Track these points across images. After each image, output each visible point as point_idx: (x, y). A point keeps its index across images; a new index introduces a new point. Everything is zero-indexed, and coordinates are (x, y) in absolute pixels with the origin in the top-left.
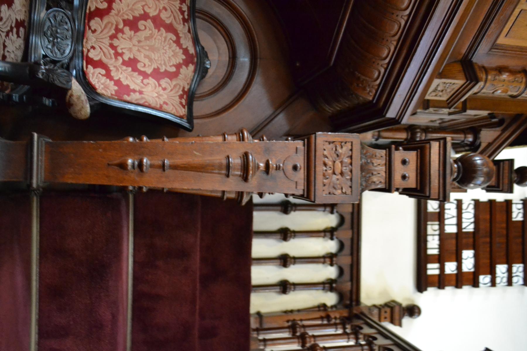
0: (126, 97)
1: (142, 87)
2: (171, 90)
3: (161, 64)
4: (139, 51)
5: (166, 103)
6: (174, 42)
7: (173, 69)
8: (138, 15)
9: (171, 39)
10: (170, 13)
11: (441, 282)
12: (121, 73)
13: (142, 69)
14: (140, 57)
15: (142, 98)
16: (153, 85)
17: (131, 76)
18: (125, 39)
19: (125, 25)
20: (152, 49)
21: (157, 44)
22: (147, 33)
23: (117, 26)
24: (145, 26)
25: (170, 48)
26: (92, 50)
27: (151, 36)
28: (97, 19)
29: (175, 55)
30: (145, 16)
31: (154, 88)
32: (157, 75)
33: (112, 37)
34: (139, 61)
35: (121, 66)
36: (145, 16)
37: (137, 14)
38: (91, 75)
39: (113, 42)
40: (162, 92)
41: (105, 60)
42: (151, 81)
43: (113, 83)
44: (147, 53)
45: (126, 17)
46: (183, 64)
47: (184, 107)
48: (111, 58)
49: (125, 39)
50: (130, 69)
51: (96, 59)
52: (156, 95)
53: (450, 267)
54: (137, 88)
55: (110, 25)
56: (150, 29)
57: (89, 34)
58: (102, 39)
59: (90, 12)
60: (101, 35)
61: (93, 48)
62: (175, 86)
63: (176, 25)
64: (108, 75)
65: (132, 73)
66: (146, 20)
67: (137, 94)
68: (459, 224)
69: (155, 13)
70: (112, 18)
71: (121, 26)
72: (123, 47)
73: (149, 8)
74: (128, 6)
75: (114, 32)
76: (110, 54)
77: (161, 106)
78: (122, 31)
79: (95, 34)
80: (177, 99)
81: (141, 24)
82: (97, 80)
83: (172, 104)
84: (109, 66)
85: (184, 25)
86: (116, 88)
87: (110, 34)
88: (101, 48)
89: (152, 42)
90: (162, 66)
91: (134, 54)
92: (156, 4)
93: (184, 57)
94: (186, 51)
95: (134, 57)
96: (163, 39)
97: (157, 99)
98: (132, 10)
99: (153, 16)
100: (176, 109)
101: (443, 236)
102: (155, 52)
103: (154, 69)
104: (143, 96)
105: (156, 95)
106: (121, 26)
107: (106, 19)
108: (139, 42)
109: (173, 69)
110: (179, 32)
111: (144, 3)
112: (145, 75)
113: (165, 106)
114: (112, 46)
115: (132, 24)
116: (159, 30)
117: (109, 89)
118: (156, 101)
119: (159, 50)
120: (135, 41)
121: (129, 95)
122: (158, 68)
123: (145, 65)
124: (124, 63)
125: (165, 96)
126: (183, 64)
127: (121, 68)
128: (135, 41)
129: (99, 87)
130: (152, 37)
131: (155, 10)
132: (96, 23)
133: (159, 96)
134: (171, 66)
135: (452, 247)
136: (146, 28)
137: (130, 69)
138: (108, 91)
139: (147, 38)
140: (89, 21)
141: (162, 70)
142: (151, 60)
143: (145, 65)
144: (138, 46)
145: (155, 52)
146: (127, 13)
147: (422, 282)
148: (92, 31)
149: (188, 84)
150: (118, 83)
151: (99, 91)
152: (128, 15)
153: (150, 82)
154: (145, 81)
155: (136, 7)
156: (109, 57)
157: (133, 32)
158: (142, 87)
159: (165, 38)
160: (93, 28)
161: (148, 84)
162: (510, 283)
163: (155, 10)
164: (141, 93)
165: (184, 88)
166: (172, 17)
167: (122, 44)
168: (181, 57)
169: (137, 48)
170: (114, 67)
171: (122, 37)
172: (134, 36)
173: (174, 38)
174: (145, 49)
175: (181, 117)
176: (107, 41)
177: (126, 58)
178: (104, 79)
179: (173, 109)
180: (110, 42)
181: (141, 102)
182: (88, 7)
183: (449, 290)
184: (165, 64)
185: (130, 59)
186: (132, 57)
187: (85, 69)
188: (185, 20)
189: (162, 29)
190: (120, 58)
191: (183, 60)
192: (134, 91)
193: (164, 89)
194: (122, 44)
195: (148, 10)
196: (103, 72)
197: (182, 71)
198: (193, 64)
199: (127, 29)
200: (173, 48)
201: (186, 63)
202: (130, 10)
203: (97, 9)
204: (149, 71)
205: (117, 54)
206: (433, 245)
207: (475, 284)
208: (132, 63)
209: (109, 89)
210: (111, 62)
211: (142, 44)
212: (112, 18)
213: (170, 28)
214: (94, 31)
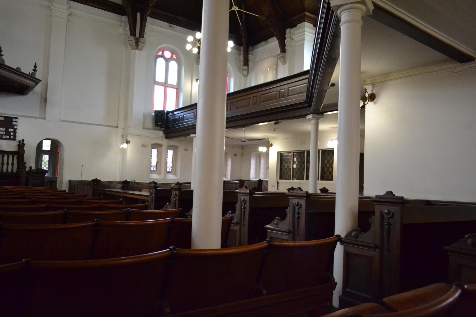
11: (15, 136)
53: (12, 134)
68: (3, 131)
101: (6, 135)
135: (8, 133)
147: (14, 139)
162: (16, 122)
183: (17, 134)
206: (7, 137)
207: (16, 129)
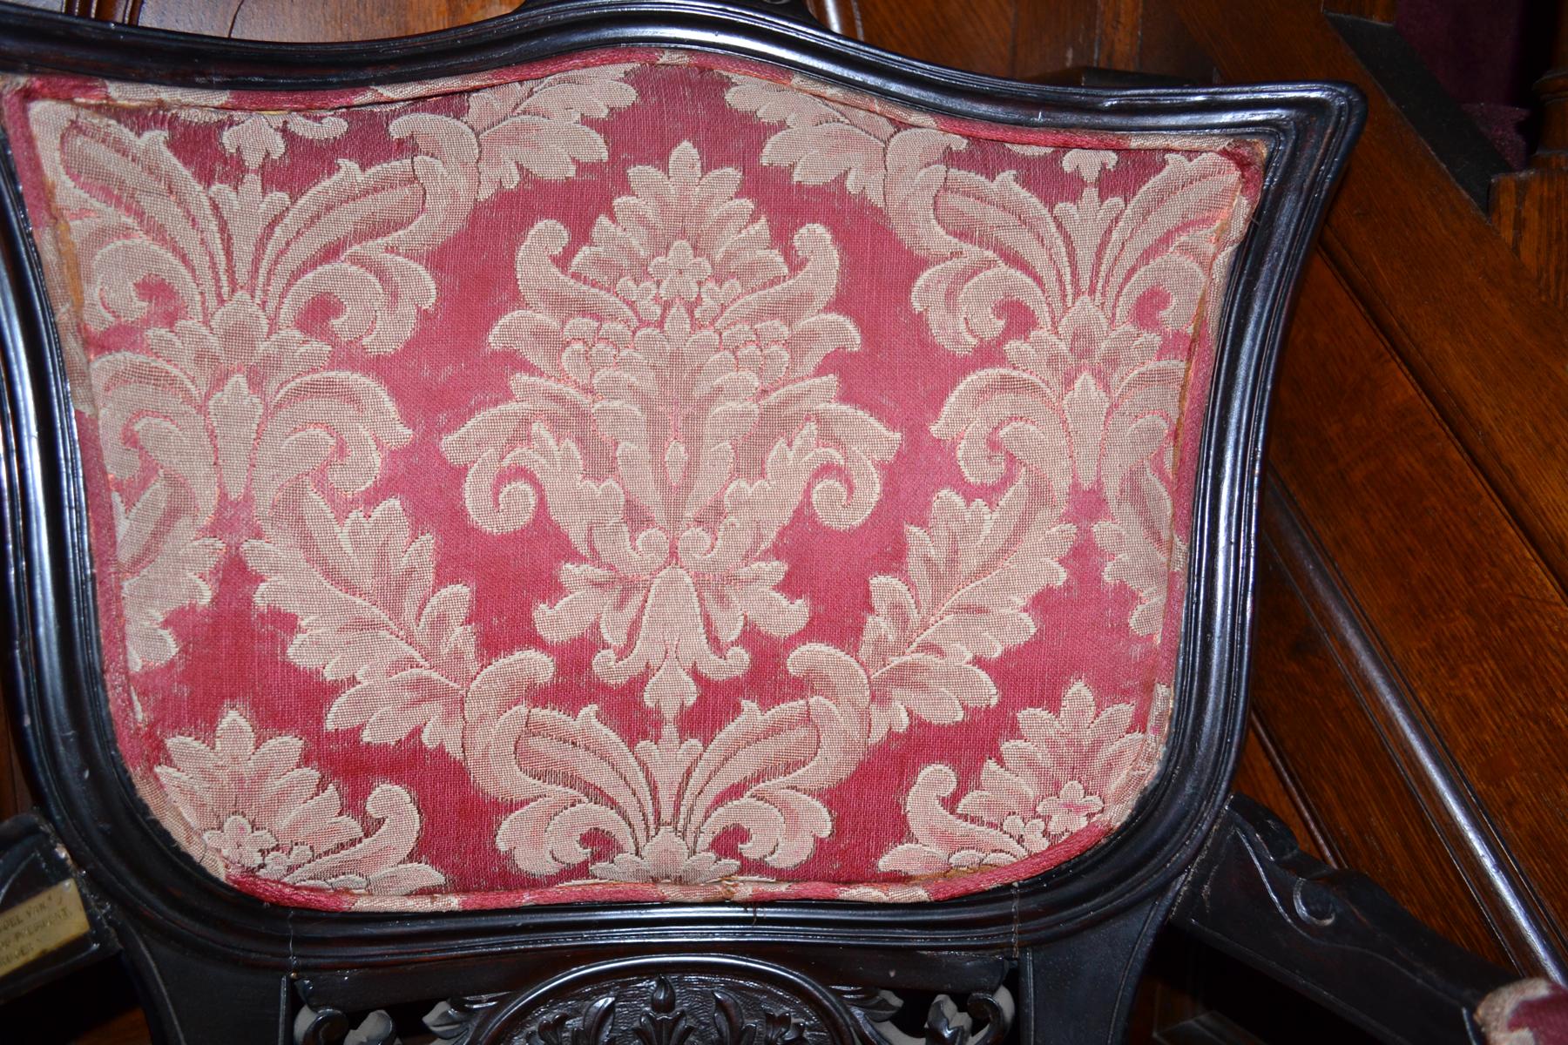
0: (1150, 617)
1: (1040, 493)
2: (1013, 259)
4: (712, 516)
5: (1148, 308)
6: (581, 234)
7: (814, 237)
8: (428, 541)
9: (563, 261)
10: (342, 265)
12: (927, 647)
13: (871, 492)
14: (768, 500)
15: (1134, 491)
16: (1003, 404)
17: (943, 575)
18: (634, 627)
21: (627, 377)
22: (552, 454)
23: (541, 696)
24: (503, 478)
25: (641, 271)
26: (750, 850)
27: (573, 421)
30: (425, 486)
31: (1027, 399)
33: (630, 713)
34: (803, 514)
35: (865, 651)
36: (425, 486)
37: (419, 552)
38: (962, 857)
39: (670, 711)
42: (960, 418)
44: (719, 451)
45: (461, 636)
46: (747, 158)
47: (1141, 166)
48: (807, 718)
49: (634, 627)
52: (1085, 379)
55: (538, 744)
56: (521, 435)
57: (616, 873)
58: (654, 790)
60: (624, 798)
61: (729, 842)
63: (438, 221)
64: (971, 744)
65: (914, 564)
67: (1102, 530)
70: (487, 732)
73: (341, 450)
74: (372, 625)
75: (590, 710)
76: (774, 730)
78: (575, 658)
79: (622, 834)
80: (1087, 214)
81: (495, 511)
82: (1014, 823)
83: (1147, 255)
84: (878, 735)
85: (406, 147)
88: (736, 791)
89: (620, 417)
90: (811, 336)
91: (747, 558)
92: (298, 394)
94: (634, 137)
95: (777, 552)
96: (584, 324)
97: (1124, 377)
98: (392, 593)
99: (409, 421)
100: (1185, 226)
102: (702, 389)
103: (845, 398)
104: (1112, 489)
105: (1085, 379)
106: (540, 666)
107: (499, 775)
108: (636, 517)
109: (814, 237)
110: (485, 193)
111: (315, 501)
112: (916, 474)
113: (1177, 315)
114: (710, 710)
117: (1097, 744)
118: (1144, 380)
119: (676, 357)
120: (637, 552)
121: (1125, 598)
122: (835, 363)
123: (826, 470)
124: (840, 619)
125: (1085, 309)
126: (747, 158)
127: (882, 651)
129: (1071, 807)
130: (583, 416)
131: (351, 397)
132: (536, 841)
134: (796, 265)
136: (521, 473)
138: (1109, 750)
139: (600, 462)
141: (853, 337)
142: (775, 424)
143: (826, 470)
144: (675, 520)
145: (702, 389)
146: (421, 630)
148: (597, 857)
149: (900, 126)
150: (1027, 678)
151: (1117, 815)
152: (440, 623)
153: (977, 427)
155: (358, 564)
156: (802, 732)
158: (1040, 493)
160: (580, 854)
161: (994, 445)
163: (351, 397)
164: (1088, 504)
165: (951, 158)
166: (374, 248)
170: (879, 697)
171: (622, 654)
172: (595, 557)
173: (546, 235)
174: (691, 467)
176: (669, 755)
177: (795, 613)
179: (1185, 249)
180: (669, 731)
182: (424, 905)
185: (789, 587)
186: (777, 569)
187: (921, 894)
188: (370, 142)
189: (495, 339)
190: (799, 660)
192: (1082, 556)
193: (1019, 319)
196: (935, 778)
198: (726, 84)
199: (556, 620)
200: (637, 242)
201: (733, 139)
202: (395, 611)
204: (873, 439)
205: (768, 675)
208: (832, 576)
209: (1097, 744)
210: (844, 719)
211: (651, 497)
212: (479, 739)
213: (475, 268)
214: (600, 843)
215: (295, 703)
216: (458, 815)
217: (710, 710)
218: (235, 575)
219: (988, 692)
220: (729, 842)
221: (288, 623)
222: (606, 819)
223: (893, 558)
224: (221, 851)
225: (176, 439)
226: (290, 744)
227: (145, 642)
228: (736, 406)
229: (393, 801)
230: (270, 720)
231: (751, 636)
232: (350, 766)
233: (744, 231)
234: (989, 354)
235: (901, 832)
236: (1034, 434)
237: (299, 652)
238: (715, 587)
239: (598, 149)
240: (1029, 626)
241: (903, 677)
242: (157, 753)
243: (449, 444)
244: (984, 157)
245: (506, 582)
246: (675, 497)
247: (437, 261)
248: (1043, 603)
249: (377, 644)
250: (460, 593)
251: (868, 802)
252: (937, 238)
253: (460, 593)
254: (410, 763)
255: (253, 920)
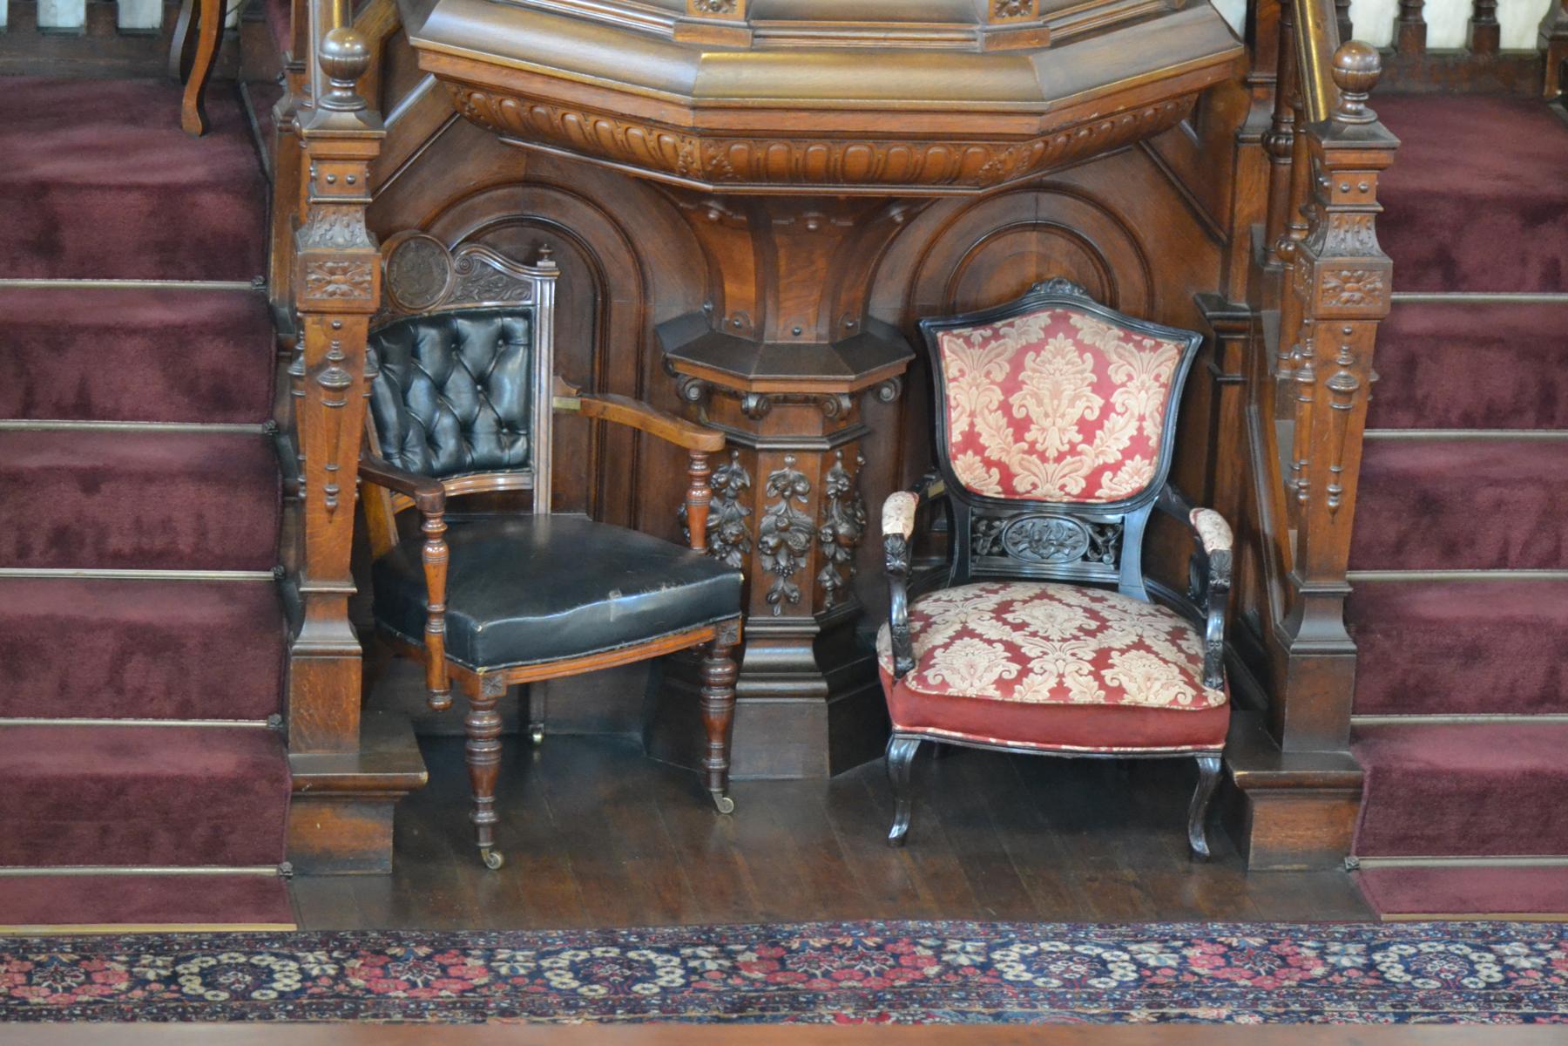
0: (1153, 442)
3: (1083, 380)
5: (1157, 378)
6: (1038, 355)
7: (1088, 356)
14: (1075, 414)
17: (1112, 431)
19: (1023, 440)
20: (1056, 394)
23: (1025, 452)
25: (1050, 362)
27: (1035, 395)
28: (1015, 482)
29: (1060, 352)
30: (1005, 408)
32: (1103, 387)
33: (1043, 457)
36: (1005, 408)
40: (1136, 383)
41: (1085, 471)
42: (1117, 398)
43: (1128, 462)
44: (1065, 402)
45: (1010, 439)
47: (1158, 345)
50: (1099, 433)
51: (1083, 484)
54: (1135, 424)
56: (1024, 398)
57: (1037, 493)
59: (1004, 492)
61: (1062, 488)
62: (1121, 356)
63: (1008, 354)
66: (1011, 406)
67: (1145, 424)
69: (998, 391)
70: (1014, 460)
71: (1025, 446)
72: (1058, 443)
77: (1164, 385)
78: (1033, 444)
80: (1146, 355)
81: (1018, 414)
85: (1004, 337)
86: (1138, 457)
87: (1038, 462)
89: (1045, 393)
93: (1061, 335)
94: (1050, 332)
98: (998, 429)
103: (1094, 391)
106: (1025, 446)
107: (1015, 469)
108: (1046, 415)
109: (1088, 356)
112: (1107, 409)
113: (1163, 379)
114: (1060, 458)
115: (1020, 427)
116: (1024, 382)
120: (1047, 423)
121: (1148, 438)
124: (1089, 439)
125: (1144, 376)
128: (1047, 423)
133: (1143, 386)
137: (1099, 433)
139: (1040, 403)
140: (1016, 493)
141: (1094, 378)
150: (1128, 454)
151: (1145, 484)
154: (1119, 409)
157: (1033, 427)
158: (1132, 415)
159: (1034, 371)
164: (1142, 418)
165: (1120, 339)
167: (1053, 443)
168: (1060, 341)
169: (1059, 420)
173: (1031, 355)
175: (1182, 353)
176: (1051, 467)
177: (1080, 437)
178: (1123, 475)
181: (1158, 418)
184: (1082, 372)
185: (1079, 432)
188: (997, 336)
189: (1020, 378)
190: (1081, 447)
191: (1067, 337)
192: (1140, 429)
193: (1130, 377)
194: (1053, 443)
195: (995, 404)
196: (1108, 475)
197: (1088, 341)
199: (1029, 436)
201: (1072, 332)
203: (999, 483)
204: (1098, 402)
208: (1088, 429)
210: (1090, 458)
211: (1050, 411)
213: (1017, 365)
215: (980, 450)
216: (1007, 477)
217: (1060, 458)
218: (972, 425)
219: (1120, 457)
220: (1062, 488)
221: (979, 435)
222: (1036, 480)
223: (1101, 427)
224: (964, 478)
225: (962, 399)
226: (978, 458)
227: (956, 436)
228: (1068, 393)
229: (995, 471)
230: (976, 453)
231: (1070, 442)
232: (988, 463)
233: (1073, 355)
234: (1123, 385)
235: (1100, 487)
236: (1132, 403)
237: (982, 440)
238: (1062, 431)
239: (1042, 335)
240: (1128, 443)
241: (1102, 452)
242: (955, 458)
243: (1011, 400)
244: (1127, 339)
245: (1020, 427)
246: (1055, 411)
247: (1010, 361)
248: (1131, 438)
249: (996, 439)
250: (1011, 430)
251: (1093, 480)
252: (1114, 358)
253: (1011, 430)
254: (999, 464)
255: (967, 494)
